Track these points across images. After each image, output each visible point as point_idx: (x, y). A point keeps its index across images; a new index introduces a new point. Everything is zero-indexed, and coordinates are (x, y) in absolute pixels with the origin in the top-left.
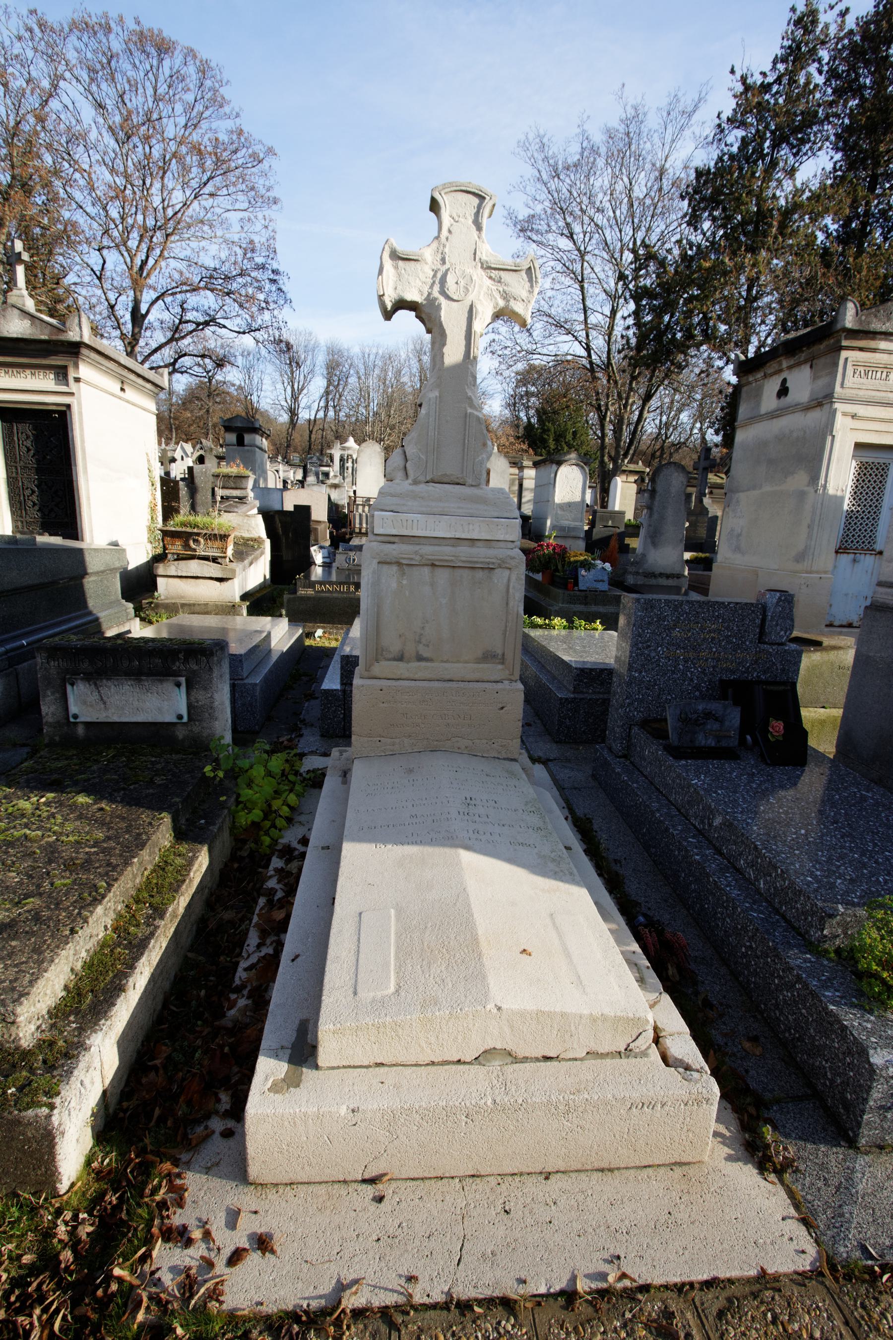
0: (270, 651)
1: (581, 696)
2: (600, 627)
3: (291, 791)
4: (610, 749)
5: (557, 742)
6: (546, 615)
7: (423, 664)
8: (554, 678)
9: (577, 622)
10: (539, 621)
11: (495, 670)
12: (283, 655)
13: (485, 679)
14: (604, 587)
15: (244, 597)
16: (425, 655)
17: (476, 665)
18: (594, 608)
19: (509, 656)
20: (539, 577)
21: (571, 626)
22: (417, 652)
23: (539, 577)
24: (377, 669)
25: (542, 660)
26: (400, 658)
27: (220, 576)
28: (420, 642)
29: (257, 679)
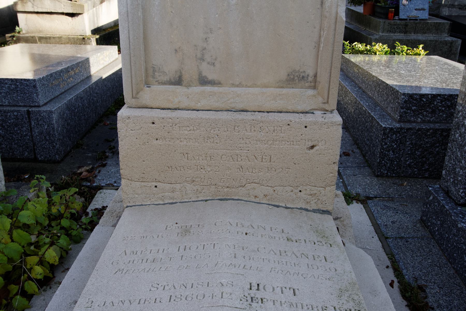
0: (90, 76)
1: (408, 126)
2: (423, 52)
3: (52, 244)
4: (447, 193)
5: (377, 176)
6: (367, 41)
7: (208, 88)
8: (376, 104)
9: (399, 47)
10: (360, 46)
11: (303, 97)
12: (101, 81)
13: (290, 108)
14: (424, 15)
15: (95, 31)
16: (211, 77)
17: (278, 90)
18: (413, 36)
19: (323, 78)
20: (360, 9)
21: (393, 51)
22: (200, 74)
23: (360, 9)
24: (147, 96)
25: (363, 86)
26: (178, 81)
27: (71, 11)
28: (202, 59)
29: (55, 107)
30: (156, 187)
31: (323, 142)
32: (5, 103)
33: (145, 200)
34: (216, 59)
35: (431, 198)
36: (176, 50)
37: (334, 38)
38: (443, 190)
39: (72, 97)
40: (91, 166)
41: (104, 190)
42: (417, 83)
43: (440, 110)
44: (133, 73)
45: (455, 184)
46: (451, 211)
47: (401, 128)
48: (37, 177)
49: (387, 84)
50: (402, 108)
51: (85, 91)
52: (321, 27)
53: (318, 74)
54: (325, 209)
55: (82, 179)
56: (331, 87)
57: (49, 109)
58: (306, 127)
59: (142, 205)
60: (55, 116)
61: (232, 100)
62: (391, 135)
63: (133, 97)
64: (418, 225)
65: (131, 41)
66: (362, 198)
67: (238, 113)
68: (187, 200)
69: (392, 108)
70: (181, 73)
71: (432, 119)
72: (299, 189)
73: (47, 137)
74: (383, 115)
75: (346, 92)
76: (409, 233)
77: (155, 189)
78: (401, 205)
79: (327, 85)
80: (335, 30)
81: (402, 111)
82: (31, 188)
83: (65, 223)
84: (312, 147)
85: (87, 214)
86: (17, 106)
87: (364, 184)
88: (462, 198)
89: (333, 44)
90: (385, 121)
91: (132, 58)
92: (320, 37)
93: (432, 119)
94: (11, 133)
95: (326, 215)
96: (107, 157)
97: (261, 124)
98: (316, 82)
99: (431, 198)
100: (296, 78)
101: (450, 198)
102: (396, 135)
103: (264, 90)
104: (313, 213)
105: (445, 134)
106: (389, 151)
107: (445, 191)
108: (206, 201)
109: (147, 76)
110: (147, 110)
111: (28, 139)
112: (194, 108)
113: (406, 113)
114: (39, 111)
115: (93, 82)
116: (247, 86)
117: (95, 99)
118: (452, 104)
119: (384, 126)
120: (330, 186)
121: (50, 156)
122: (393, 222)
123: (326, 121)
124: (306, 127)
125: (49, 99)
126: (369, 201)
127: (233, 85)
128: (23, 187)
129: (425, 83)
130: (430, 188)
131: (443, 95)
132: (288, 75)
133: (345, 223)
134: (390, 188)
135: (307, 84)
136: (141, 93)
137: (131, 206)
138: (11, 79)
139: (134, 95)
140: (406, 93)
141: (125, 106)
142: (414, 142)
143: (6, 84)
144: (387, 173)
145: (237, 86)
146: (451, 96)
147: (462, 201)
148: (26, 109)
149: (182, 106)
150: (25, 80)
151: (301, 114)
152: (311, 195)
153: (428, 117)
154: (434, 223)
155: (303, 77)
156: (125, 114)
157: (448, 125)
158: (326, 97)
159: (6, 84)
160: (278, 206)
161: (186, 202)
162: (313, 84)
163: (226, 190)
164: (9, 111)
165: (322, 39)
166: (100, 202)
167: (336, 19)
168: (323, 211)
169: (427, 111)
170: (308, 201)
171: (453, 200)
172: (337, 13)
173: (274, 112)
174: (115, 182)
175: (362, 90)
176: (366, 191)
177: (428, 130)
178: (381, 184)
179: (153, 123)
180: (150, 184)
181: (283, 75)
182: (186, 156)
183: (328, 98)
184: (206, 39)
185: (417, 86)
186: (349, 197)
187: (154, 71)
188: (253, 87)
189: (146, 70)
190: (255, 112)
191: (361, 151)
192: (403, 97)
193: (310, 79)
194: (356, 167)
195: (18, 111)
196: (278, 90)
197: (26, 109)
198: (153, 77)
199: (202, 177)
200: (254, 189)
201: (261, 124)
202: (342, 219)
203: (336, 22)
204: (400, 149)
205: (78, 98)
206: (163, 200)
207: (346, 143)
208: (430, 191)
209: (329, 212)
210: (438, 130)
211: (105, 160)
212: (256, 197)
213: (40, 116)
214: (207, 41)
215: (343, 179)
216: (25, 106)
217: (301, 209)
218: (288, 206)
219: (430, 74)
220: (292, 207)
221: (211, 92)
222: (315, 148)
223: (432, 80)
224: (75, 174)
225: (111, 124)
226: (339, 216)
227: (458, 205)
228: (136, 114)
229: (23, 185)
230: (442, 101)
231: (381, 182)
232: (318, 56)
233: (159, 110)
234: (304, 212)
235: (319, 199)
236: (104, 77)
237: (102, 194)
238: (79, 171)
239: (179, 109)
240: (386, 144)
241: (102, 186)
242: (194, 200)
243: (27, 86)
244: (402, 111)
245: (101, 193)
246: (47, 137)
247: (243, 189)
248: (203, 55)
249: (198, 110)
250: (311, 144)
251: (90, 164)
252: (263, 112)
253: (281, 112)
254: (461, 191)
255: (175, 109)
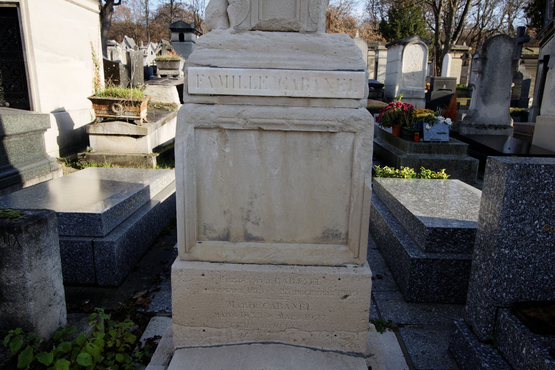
0: (150, 200)
1: (434, 256)
2: (445, 176)
4: (471, 328)
5: (408, 302)
6: (395, 165)
7: (252, 244)
8: (405, 232)
9: (424, 171)
10: (390, 170)
11: (336, 252)
12: (160, 205)
13: (325, 262)
14: (446, 138)
15: (155, 150)
16: (255, 234)
17: (315, 246)
18: (436, 157)
19: (354, 236)
20: (390, 130)
21: (418, 175)
22: (246, 231)
23: (390, 130)
24: (198, 251)
25: (393, 212)
26: (226, 238)
27: (135, 134)
28: (248, 219)
29: (116, 238)
30: (204, 330)
31: (355, 293)
32: (72, 233)
33: (194, 343)
34: (259, 220)
35: (457, 332)
36: (225, 212)
37: (363, 203)
38: (467, 324)
39: (132, 225)
40: (146, 291)
41: (157, 317)
42: (440, 214)
43: (461, 242)
44: (187, 232)
45: (478, 322)
46: (475, 349)
47: (427, 259)
48: (97, 310)
49: (414, 216)
50: (427, 240)
51: (144, 218)
52: (351, 194)
53: (350, 233)
54: (358, 352)
55: (138, 306)
56: (361, 245)
57: (111, 240)
58: (339, 279)
59: (191, 347)
60: (116, 246)
61: (273, 255)
62: (419, 265)
63: (186, 252)
64: (446, 356)
65: (186, 205)
66: (394, 325)
67: (279, 266)
68: (232, 343)
69: (418, 238)
70: (229, 230)
71: (454, 250)
72: (335, 333)
73: (108, 265)
74: (411, 244)
75: (378, 216)
76: (438, 365)
77: (203, 333)
78: (430, 333)
79: (357, 243)
80: (363, 197)
81: (427, 242)
82: (90, 321)
83: (119, 357)
84: (346, 297)
85: (140, 344)
86: (83, 236)
87: (395, 310)
88: (484, 335)
89: (362, 209)
90: (413, 251)
91: (186, 219)
92: (350, 202)
93: (454, 250)
94: (75, 261)
95: (360, 358)
96: (161, 281)
97: (300, 277)
98: (347, 239)
99: (457, 332)
100: (330, 236)
101: (474, 333)
102: (423, 265)
103: (302, 246)
104: (347, 356)
105: (467, 264)
106: (417, 279)
107: (468, 325)
108: (250, 344)
109: (199, 233)
110: (198, 263)
111: (91, 267)
112: (240, 261)
113: (431, 244)
114: (103, 242)
115: (152, 207)
116: (287, 242)
117: (153, 223)
118: (471, 237)
119: (412, 256)
120: (362, 331)
121: (109, 281)
122: (423, 353)
123: (357, 274)
124: (339, 279)
125: (112, 229)
126: (401, 329)
127: (274, 241)
128: (83, 319)
129: (447, 214)
130: (456, 322)
131: (463, 229)
132: (323, 233)
133: (378, 360)
134: (420, 315)
135: (339, 241)
136: (193, 248)
137: (181, 348)
138: (80, 213)
139: (187, 250)
140: (431, 226)
141: (178, 259)
142: (439, 271)
143: (75, 217)
144: (416, 299)
145: (278, 242)
146: (470, 229)
147: (484, 338)
148: (90, 240)
149: (229, 260)
150: (91, 214)
151: (335, 268)
152: (345, 339)
153: (451, 248)
154: (460, 357)
155: (336, 235)
156: (178, 267)
157: (469, 255)
158: (357, 253)
159: (75, 217)
160: (315, 350)
161: (231, 345)
162: (345, 241)
163: (268, 334)
164: (75, 242)
165: (352, 204)
166: (153, 331)
167: (364, 188)
168: (356, 353)
169: (450, 243)
170: (342, 344)
171: (477, 336)
172: (364, 184)
173: (311, 265)
174: (167, 308)
175: (392, 214)
176: (397, 318)
177: (451, 261)
178: (411, 310)
179: (203, 275)
180: (199, 328)
181: (318, 233)
182: (232, 304)
183: (359, 253)
184: (251, 203)
185: (440, 218)
186: (382, 325)
187: (205, 229)
188: (292, 243)
189: (198, 228)
190: (294, 265)
191: (393, 274)
192: (427, 230)
193: (342, 236)
194: (388, 291)
195: (83, 242)
196: (314, 245)
197: (90, 240)
198: (205, 234)
199: (246, 322)
200: (294, 333)
201: (300, 277)
202: (375, 356)
203: (364, 191)
204: (427, 278)
205: (139, 225)
206: (210, 343)
207: (379, 265)
208: (455, 325)
209: (362, 354)
210: (461, 260)
211: (160, 284)
212: (295, 340)
213: (103, 246)
214: (252, 205)
215: (376, 304)
216: (90, 237)
217: (336, 351)
218: (324, 349)
219: (452, 203)
220: (328, 349)
221: (255, 247)
222: (348, 297)
223: (454, 210)
224: (131, 299)
225: (166, 244)
226: (372, 353)
227: (481, 341)
228: (188, 268)
229: (83, 317)
230: (462, 235)
231: (411, 307)
232: (349, 217)
233: (209, 263)
234: (340, 356)
235: (352, 343)
236: (162, 201)
237: (155, 322)
238: (135, 297)
239: (227, 263)
240: (414, 273)
241: (156, 313)
242: (238, 343)
243: (93, 219)
244: (427, 242)
245: (154, 320)
246: (108, 265)
247: (283, 333)
248: (248, 216)
249: (243, 264)
250: (344, 294)
251: (145, 289)
252: (302, 265)
253: (317, 266)
254: (483, 329)
255: (223, 262)
